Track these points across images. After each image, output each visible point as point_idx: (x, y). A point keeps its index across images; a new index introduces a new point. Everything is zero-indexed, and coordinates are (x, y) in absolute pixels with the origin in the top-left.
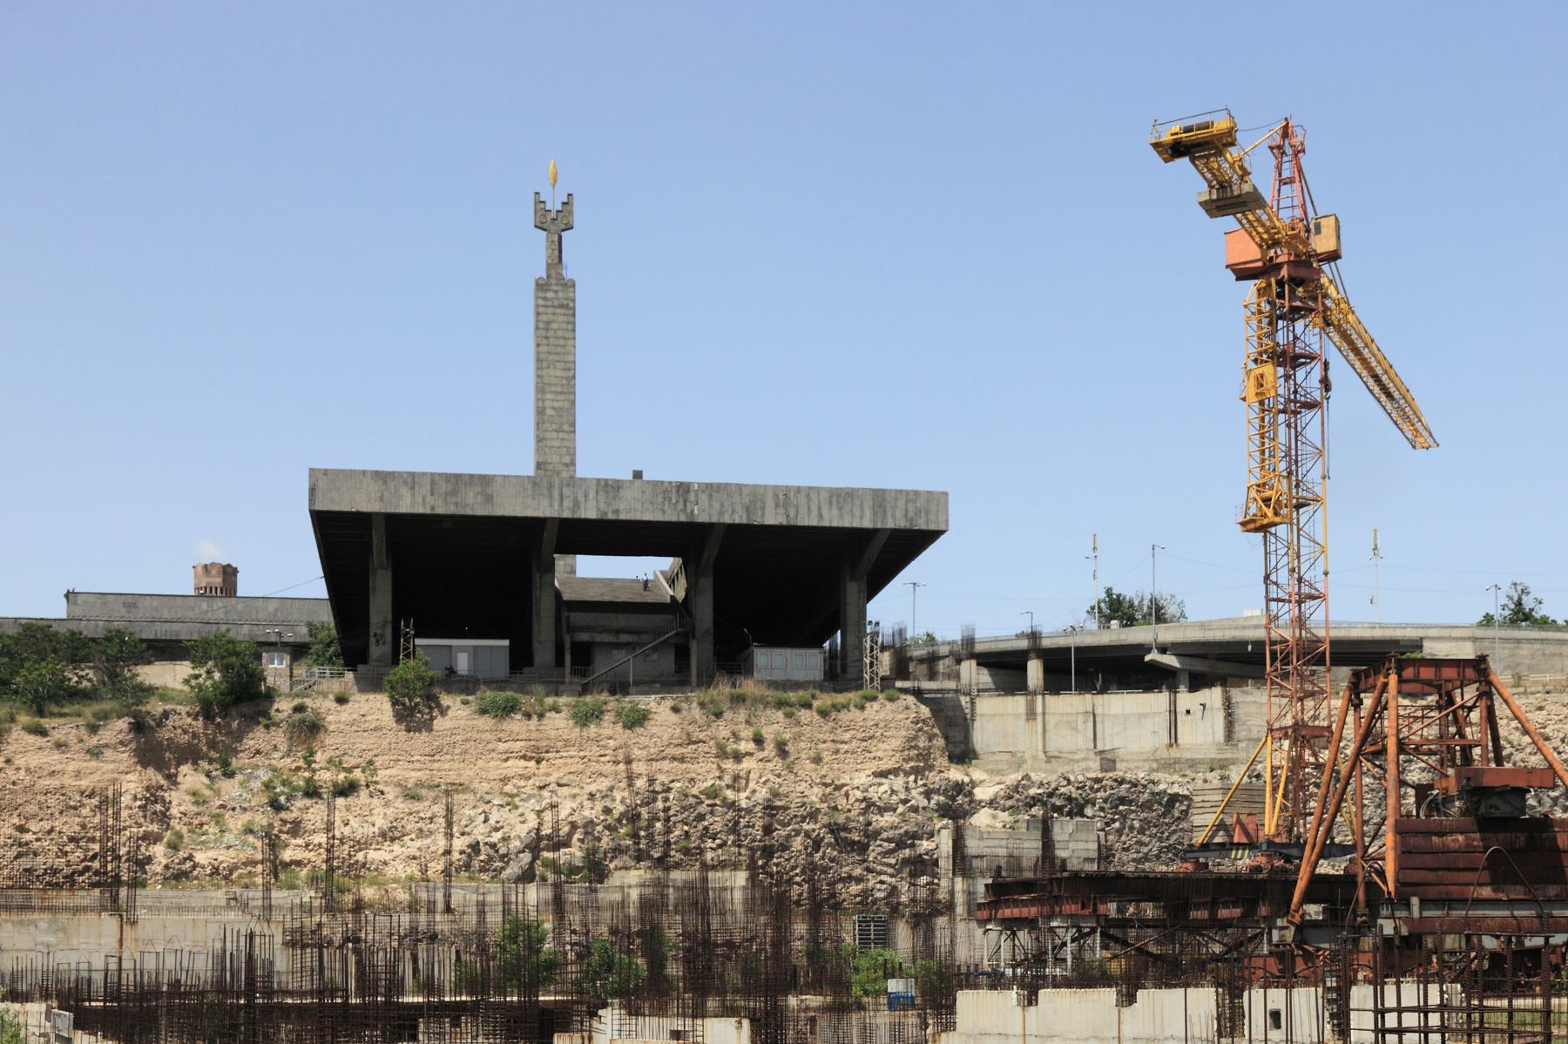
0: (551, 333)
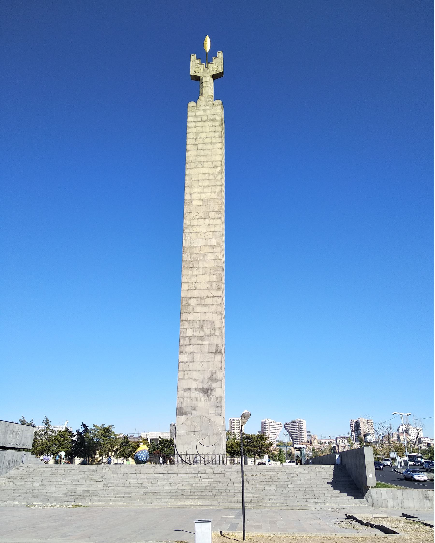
0: (199, 141)
